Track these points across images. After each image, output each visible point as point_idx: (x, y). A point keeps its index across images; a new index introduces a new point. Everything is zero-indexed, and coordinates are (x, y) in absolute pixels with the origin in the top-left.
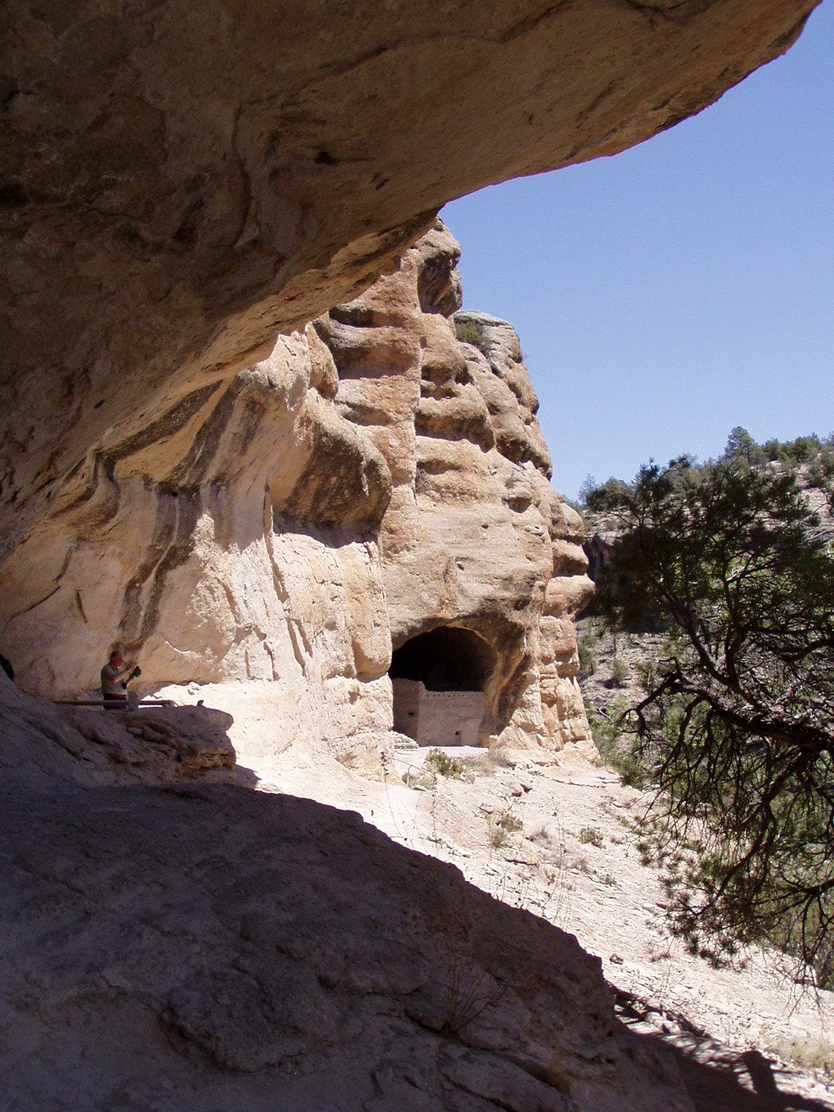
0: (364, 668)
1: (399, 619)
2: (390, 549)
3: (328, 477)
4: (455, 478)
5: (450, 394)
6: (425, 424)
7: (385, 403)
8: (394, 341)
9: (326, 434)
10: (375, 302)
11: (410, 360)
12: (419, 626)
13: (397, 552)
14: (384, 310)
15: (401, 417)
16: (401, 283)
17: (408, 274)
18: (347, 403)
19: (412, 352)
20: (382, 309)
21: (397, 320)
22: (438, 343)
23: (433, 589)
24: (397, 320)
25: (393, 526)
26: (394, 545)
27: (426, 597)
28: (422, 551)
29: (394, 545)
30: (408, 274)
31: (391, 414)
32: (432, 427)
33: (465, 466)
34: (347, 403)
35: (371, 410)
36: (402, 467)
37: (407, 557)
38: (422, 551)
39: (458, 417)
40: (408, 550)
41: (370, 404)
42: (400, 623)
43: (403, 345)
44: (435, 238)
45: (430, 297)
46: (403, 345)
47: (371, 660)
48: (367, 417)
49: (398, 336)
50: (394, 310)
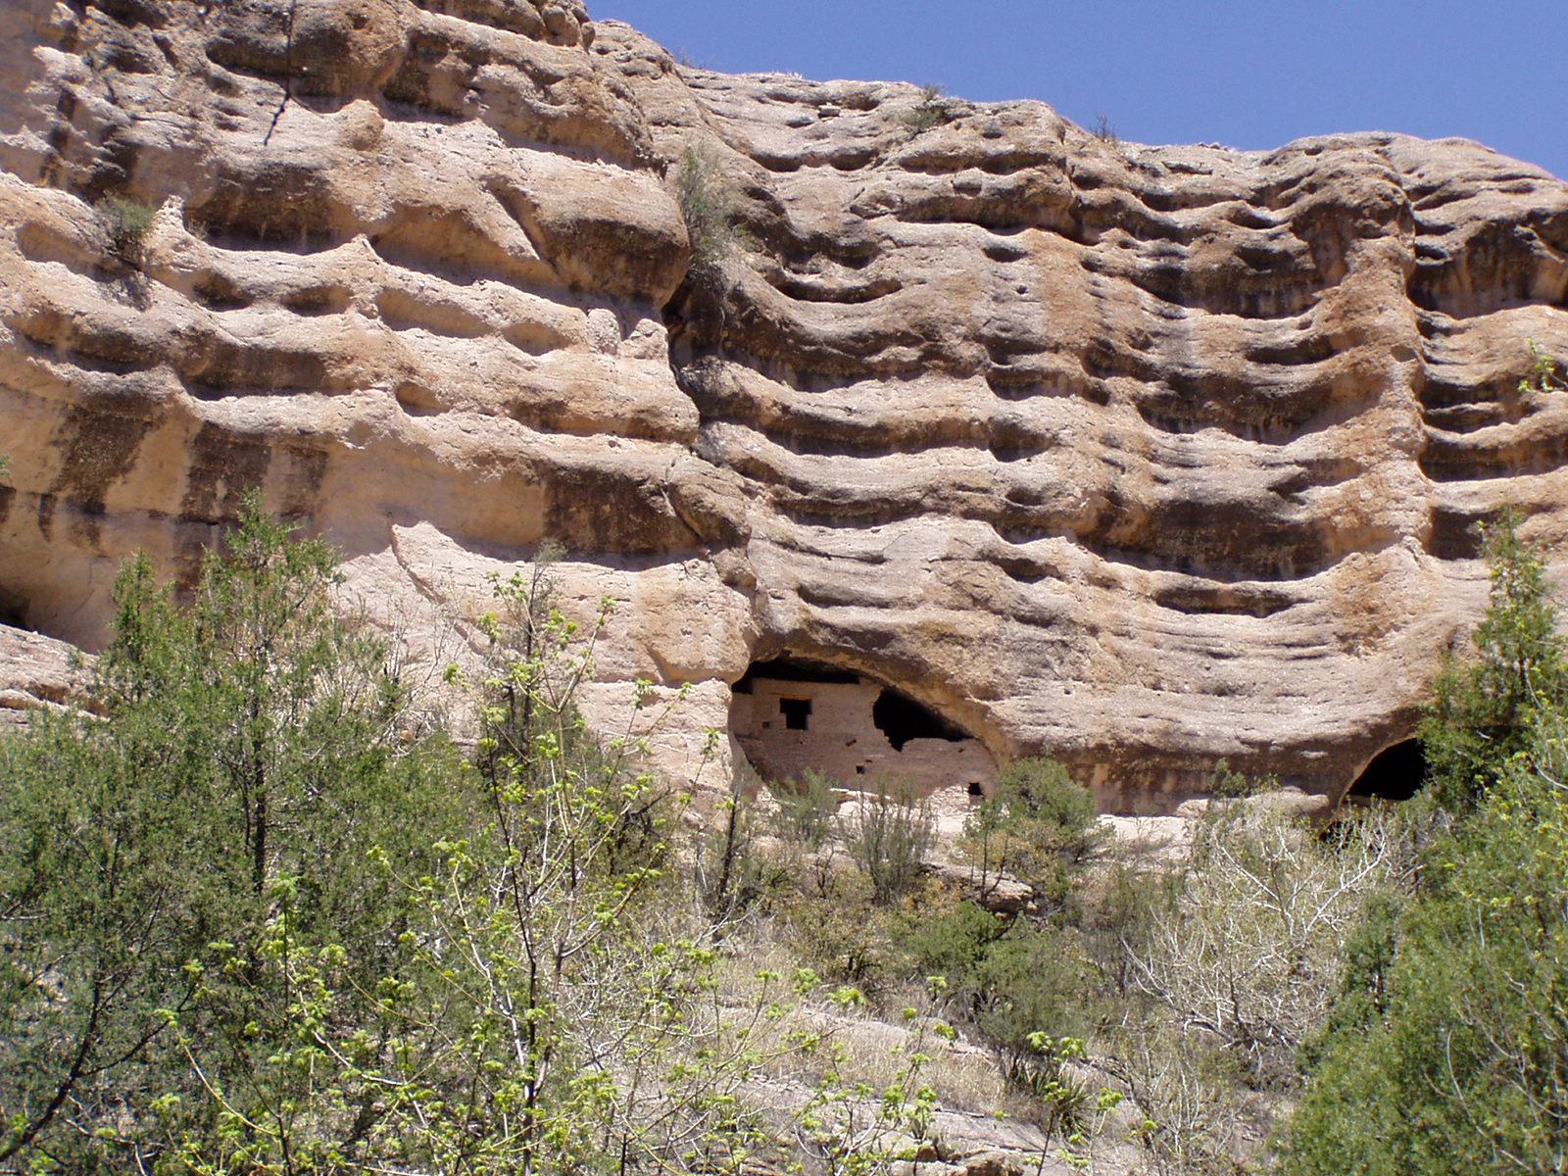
0: (675, 675)
1: (1354, 718)
2: (1370, 634)
3: (597, 508)
4: (1544, 522)
5: (1529, 410)
6: (1441, 463)
7: (1353, 447)
8: (1355, 365)
9: (563, 468)
10: (1330, 324)
11: (1382, 381)
12: (1387, 722)
13: (1381, 635)
14: (1339, 330)
15: (1374, 459)
16: (1356, 288)
17: (1366, 272)
18: (1297, 463)
19: (1380, 370)
20: (1336, 329)
21: (1356, 337)
22: (1503, 345)
23: (1417, 670)
24: (1356, 337)
25: (1374, 602)
26: (1375, 628)
27: (1402, 682)
28: (1414, 627)
29: (1375, 628)
30: (1366, 272)
31: (1360, 459)
32: (1512, 462)
33: (1561, 502)
34: (1297, 463)
35: (1336, 462)
36: (1380, 523)
37: (1395, 638)
38: (1414, 627)
39: (1540, 437)
40: (1397, 629)
41: (1332, 455)
42: (1354, 722)
43: (1366, 365)
44: (1488, 207)
45: (1512, 288)
46: (1366, 365)
47: (675, 666)
48: (1335, 473)
49: (1360, 356)
50: (1350, 325)
